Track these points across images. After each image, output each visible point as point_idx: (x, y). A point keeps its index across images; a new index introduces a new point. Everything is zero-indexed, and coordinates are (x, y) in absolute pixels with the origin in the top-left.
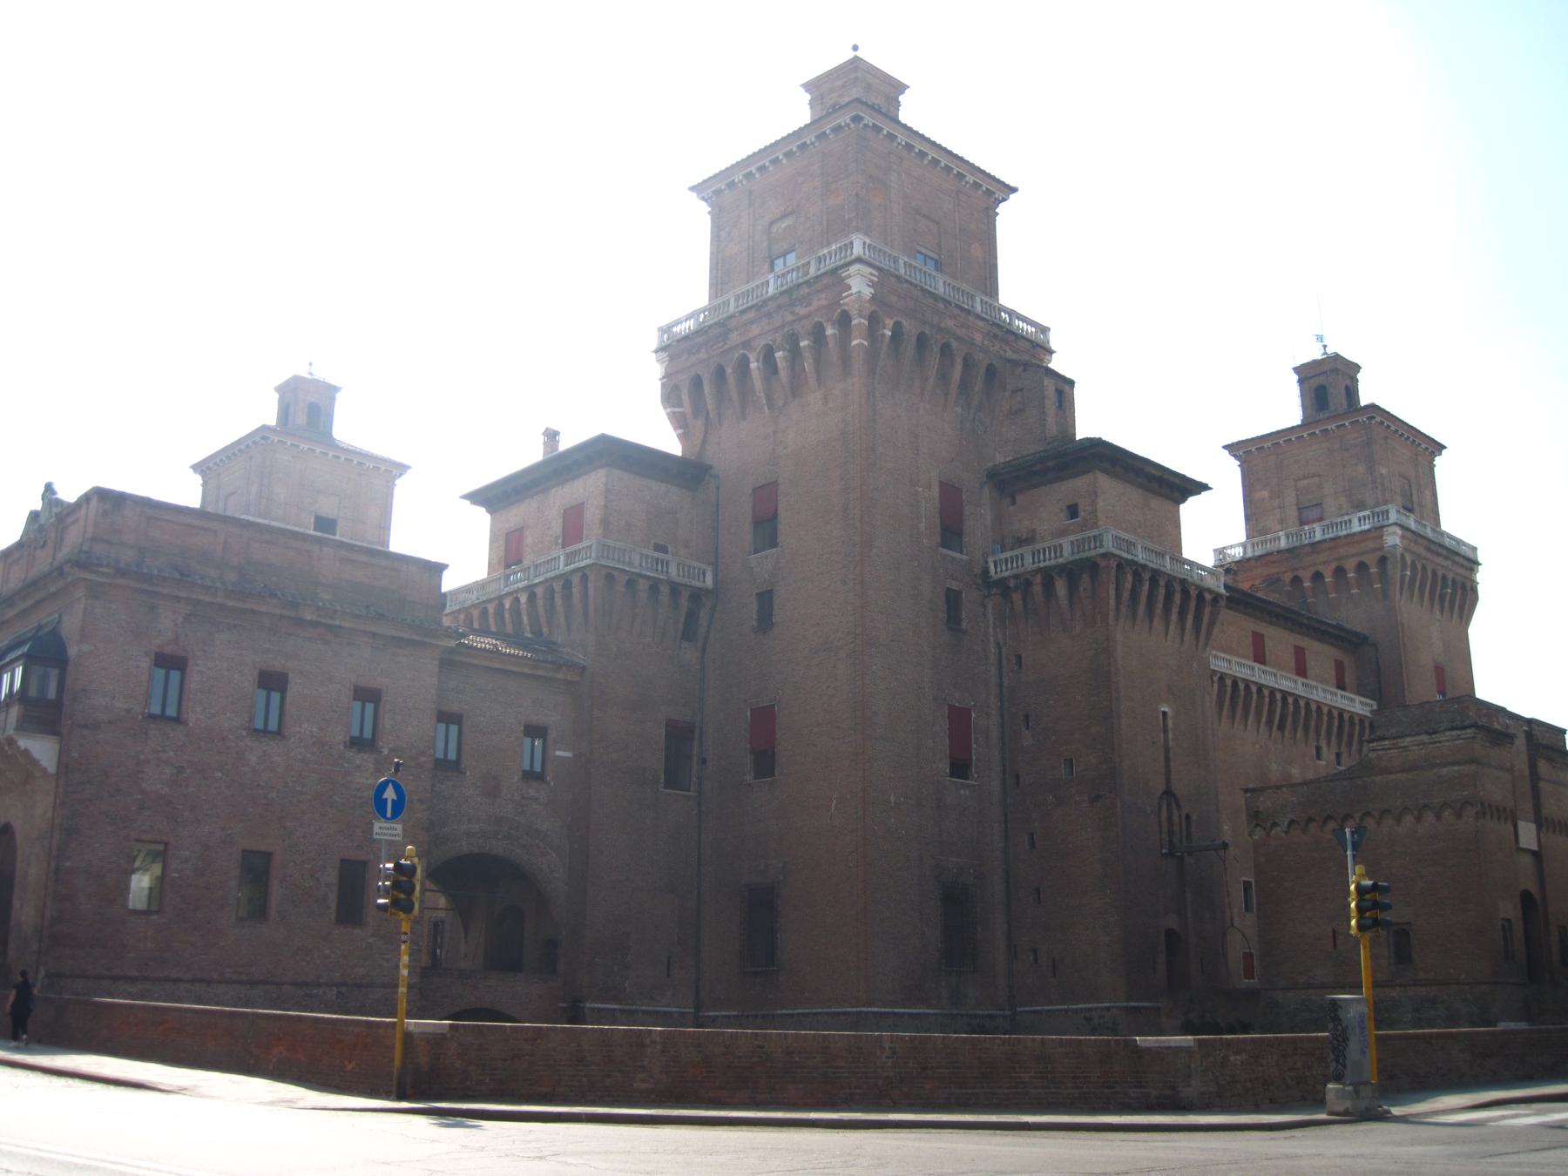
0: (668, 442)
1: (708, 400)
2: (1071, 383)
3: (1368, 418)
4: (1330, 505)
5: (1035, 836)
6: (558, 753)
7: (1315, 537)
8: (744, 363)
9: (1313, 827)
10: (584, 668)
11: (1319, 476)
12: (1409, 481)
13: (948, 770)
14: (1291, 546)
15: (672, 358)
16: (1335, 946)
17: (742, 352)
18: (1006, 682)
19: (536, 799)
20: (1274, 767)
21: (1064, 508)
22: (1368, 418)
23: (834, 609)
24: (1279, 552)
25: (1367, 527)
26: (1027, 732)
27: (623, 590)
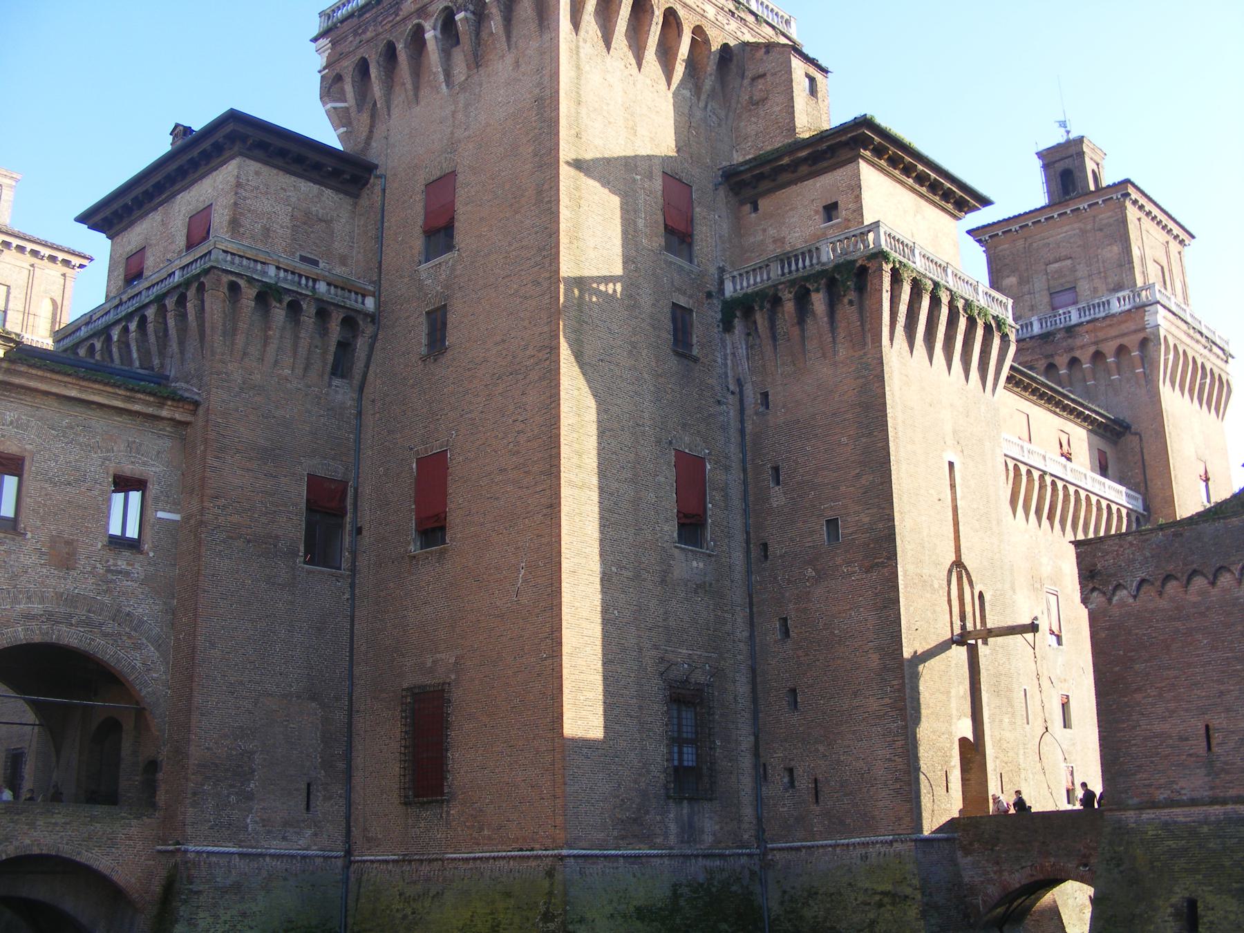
0: (327, 134)
1: (375, 85)
2: (824, 71)
3: (1122, 195)
4: (1084, 287)
5: (789, 622)
6: (161, 514)
7: (1070, 320)
8: (417, 36)
9: (1172, 587)
10: (196, 404)
11: (1071, 258)
12: (1162, 268)
13: (675, 535)
14: (1044, 330)
15: (334, 43)
16: (1209, 748)
17: (416, 21)
18: (749, 427)
19: (127, 574)
20: (1044, 560)
21: (821, 209)
22: (1122, 195)
23: (523, 320)
24: (1031, 338)
25: (1127, 307)
26: (777, 488)
27: (253, 304)
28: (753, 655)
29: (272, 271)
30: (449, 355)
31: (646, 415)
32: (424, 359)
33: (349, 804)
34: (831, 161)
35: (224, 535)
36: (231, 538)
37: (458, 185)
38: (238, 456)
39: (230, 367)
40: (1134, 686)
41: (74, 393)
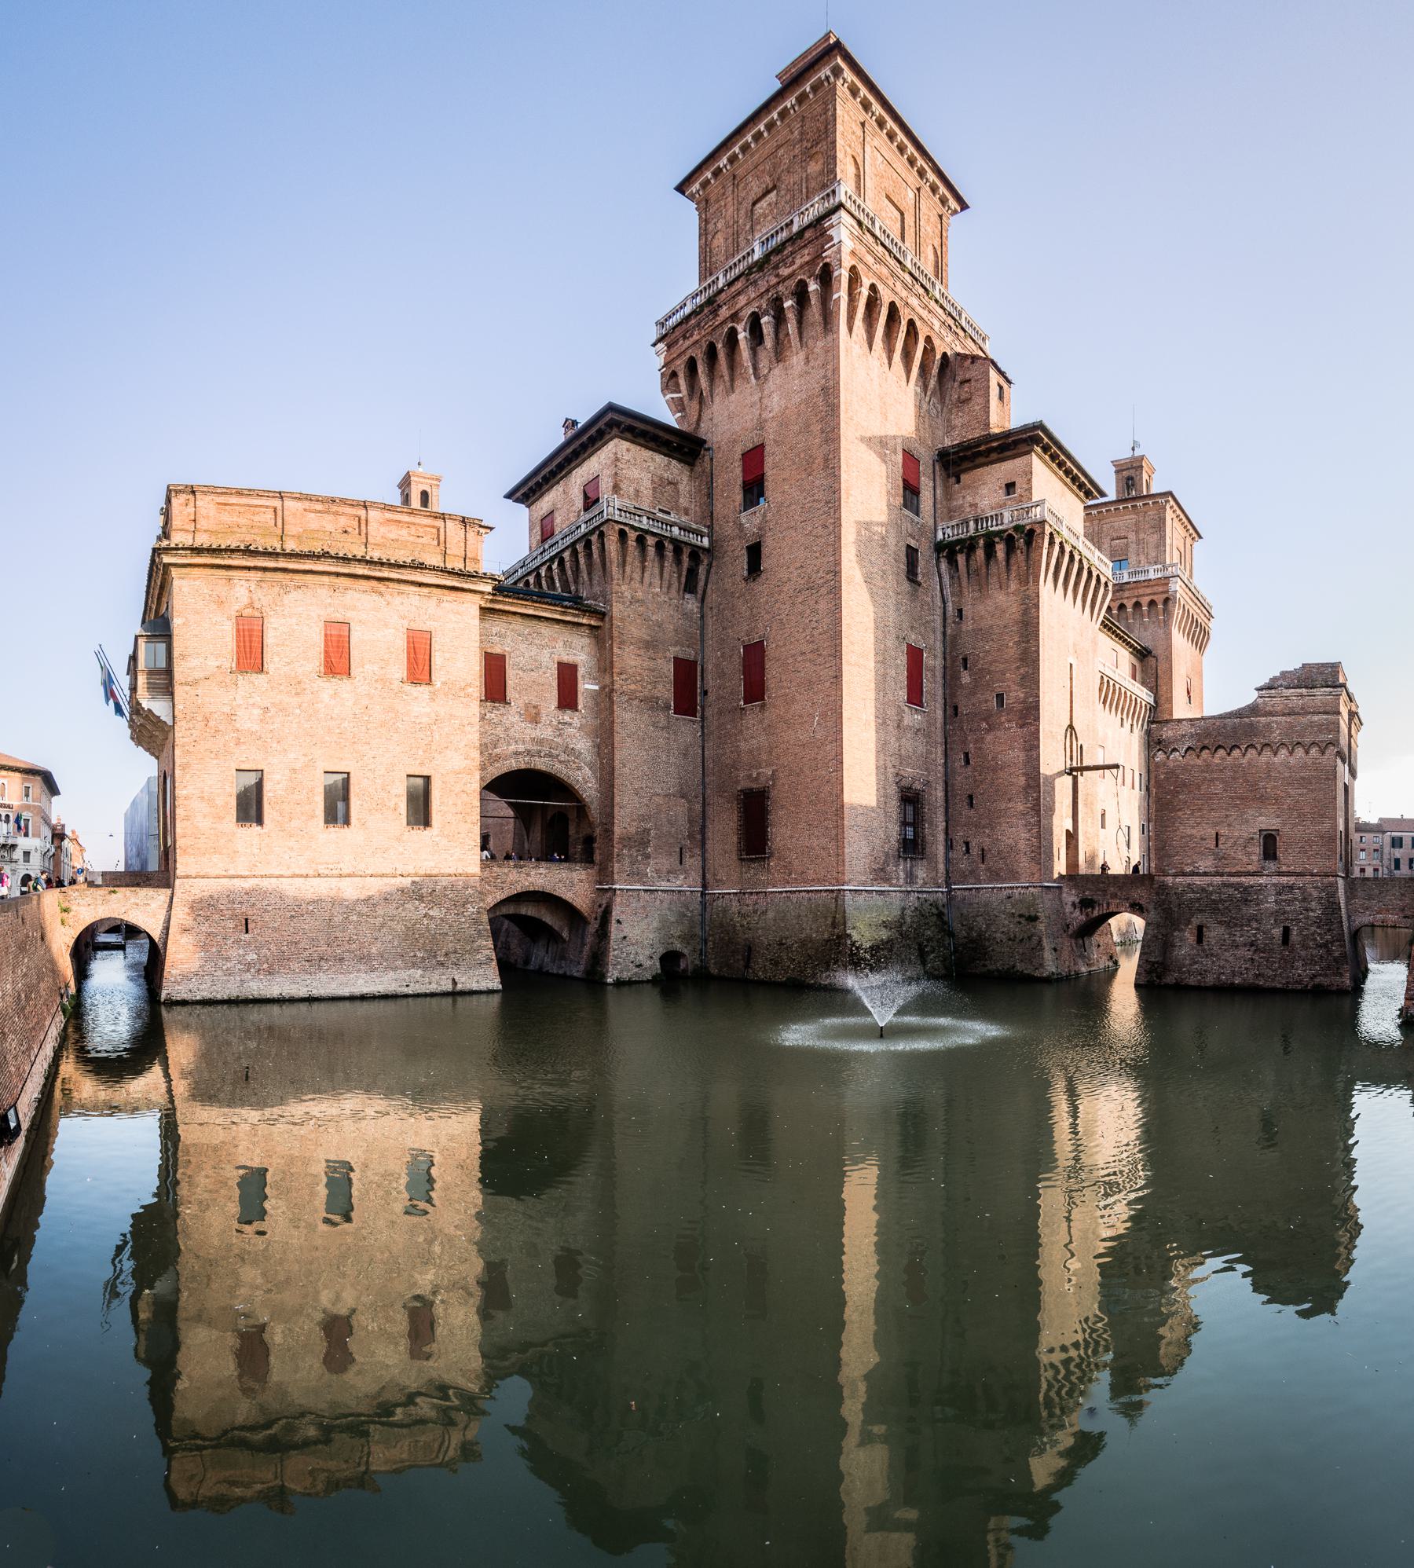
10: (604, 614)
16: (1217, 846)
27: (634, 544)
29: (645, 519)
30: (763, 576)
31: (890, 619)
32: (746, 580)
33: (704, 860)
34: (1014, 452)
35: (626, 698)
36: (630, 699)
37: (766, 454)
38: (632, 647)
39: (623, 588)
40: (1178, 807)
41: (531, 612)
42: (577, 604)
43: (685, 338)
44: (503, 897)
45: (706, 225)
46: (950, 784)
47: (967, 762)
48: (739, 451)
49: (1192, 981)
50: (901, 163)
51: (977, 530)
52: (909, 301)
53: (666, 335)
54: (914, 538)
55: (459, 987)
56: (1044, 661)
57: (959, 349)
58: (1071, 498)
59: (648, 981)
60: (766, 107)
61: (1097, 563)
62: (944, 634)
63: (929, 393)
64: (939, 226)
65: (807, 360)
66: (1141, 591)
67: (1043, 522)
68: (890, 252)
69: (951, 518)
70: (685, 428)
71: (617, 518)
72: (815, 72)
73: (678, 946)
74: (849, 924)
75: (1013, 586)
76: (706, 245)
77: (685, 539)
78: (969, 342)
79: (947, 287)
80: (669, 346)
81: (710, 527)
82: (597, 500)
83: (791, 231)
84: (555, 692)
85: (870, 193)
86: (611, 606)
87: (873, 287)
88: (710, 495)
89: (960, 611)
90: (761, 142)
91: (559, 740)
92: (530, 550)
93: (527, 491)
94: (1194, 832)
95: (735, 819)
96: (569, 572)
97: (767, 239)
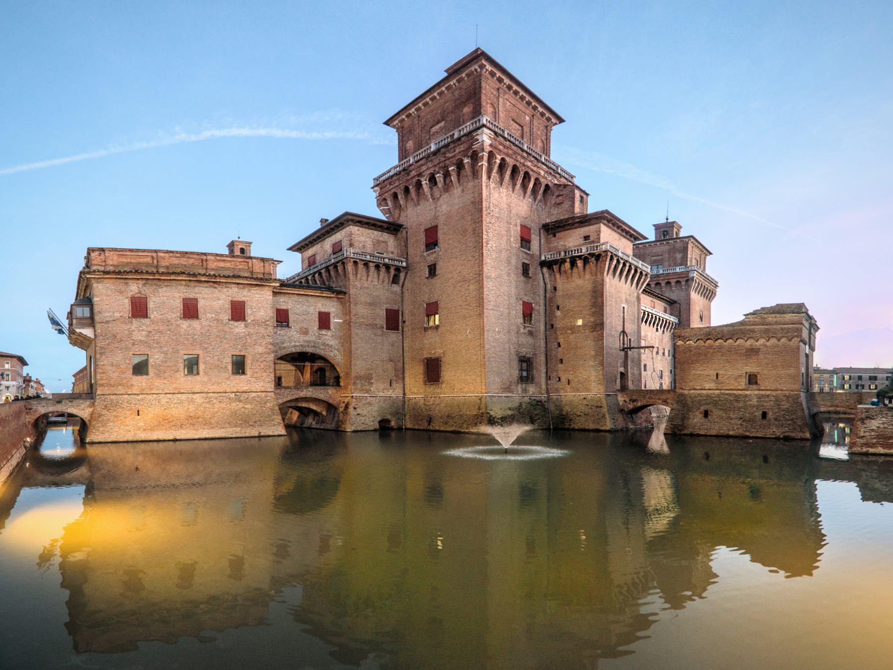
28: (546, 351)
42: (330, 289)
43: (390, 184)
44: (287, 400)
45: (403, 137)
46: (548, 354)
47: (559, 345)
48: (423, 228)
49: (702, 432)
50: (522, 106)
51: (566, 255)
52: (525, 164)
53: (379, 184)
54: (527, 260)
55: (262, 434)
56: (606, 306)
57: (556, 182)
58: (624, 241)
59: (372, 431)
60: (438, 85)
61: (640, 266)
62: (545, 297)
63: (537, 201)
64: (545, 131)
65: (463, 191)
66: (670, 277)
67: (606, 251)
68: (513, 144)
69: (550, 251)
70: (391, 220)
71: (352, 256)
72: (469, 68)
73: (389, 417)
74: (488, 409)
75: (588, 276)
76: (402, 146)
77: (393, 263)
78: (563, 180)
79: (549, 157)
80: (381, 189)
81: (407, 259)
82: (341, 250)
83: (453, 138)
84: (317, 323)
85: (501, 119)
86: (349, 290)
87: (503, 159)
88: (406, 246)
89: (555, 289)
90: (435, 101)
91: (320, 341)
92: (302, 269)
93: (300, 247)
94: (702, 372)
95: (422, 369)
96: (325, 278)
97: (439, 142)
